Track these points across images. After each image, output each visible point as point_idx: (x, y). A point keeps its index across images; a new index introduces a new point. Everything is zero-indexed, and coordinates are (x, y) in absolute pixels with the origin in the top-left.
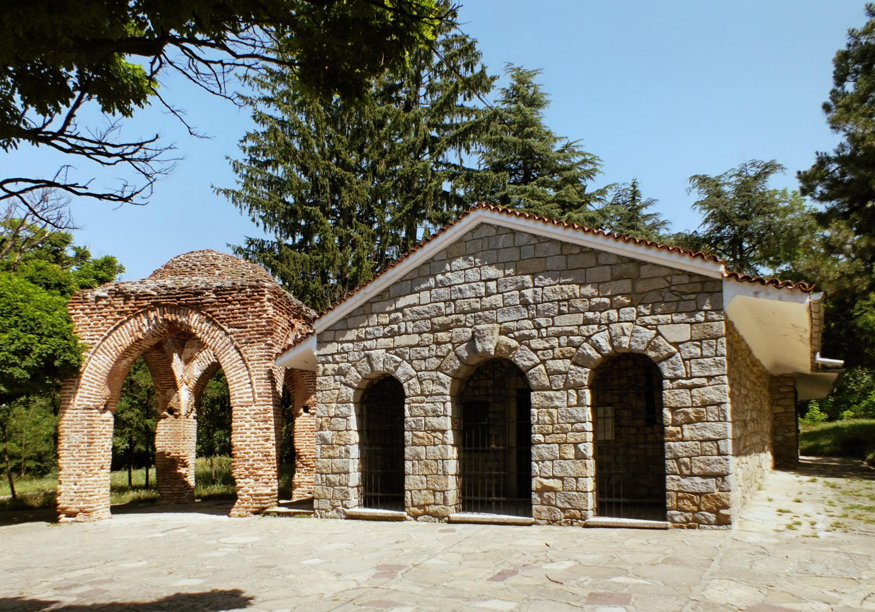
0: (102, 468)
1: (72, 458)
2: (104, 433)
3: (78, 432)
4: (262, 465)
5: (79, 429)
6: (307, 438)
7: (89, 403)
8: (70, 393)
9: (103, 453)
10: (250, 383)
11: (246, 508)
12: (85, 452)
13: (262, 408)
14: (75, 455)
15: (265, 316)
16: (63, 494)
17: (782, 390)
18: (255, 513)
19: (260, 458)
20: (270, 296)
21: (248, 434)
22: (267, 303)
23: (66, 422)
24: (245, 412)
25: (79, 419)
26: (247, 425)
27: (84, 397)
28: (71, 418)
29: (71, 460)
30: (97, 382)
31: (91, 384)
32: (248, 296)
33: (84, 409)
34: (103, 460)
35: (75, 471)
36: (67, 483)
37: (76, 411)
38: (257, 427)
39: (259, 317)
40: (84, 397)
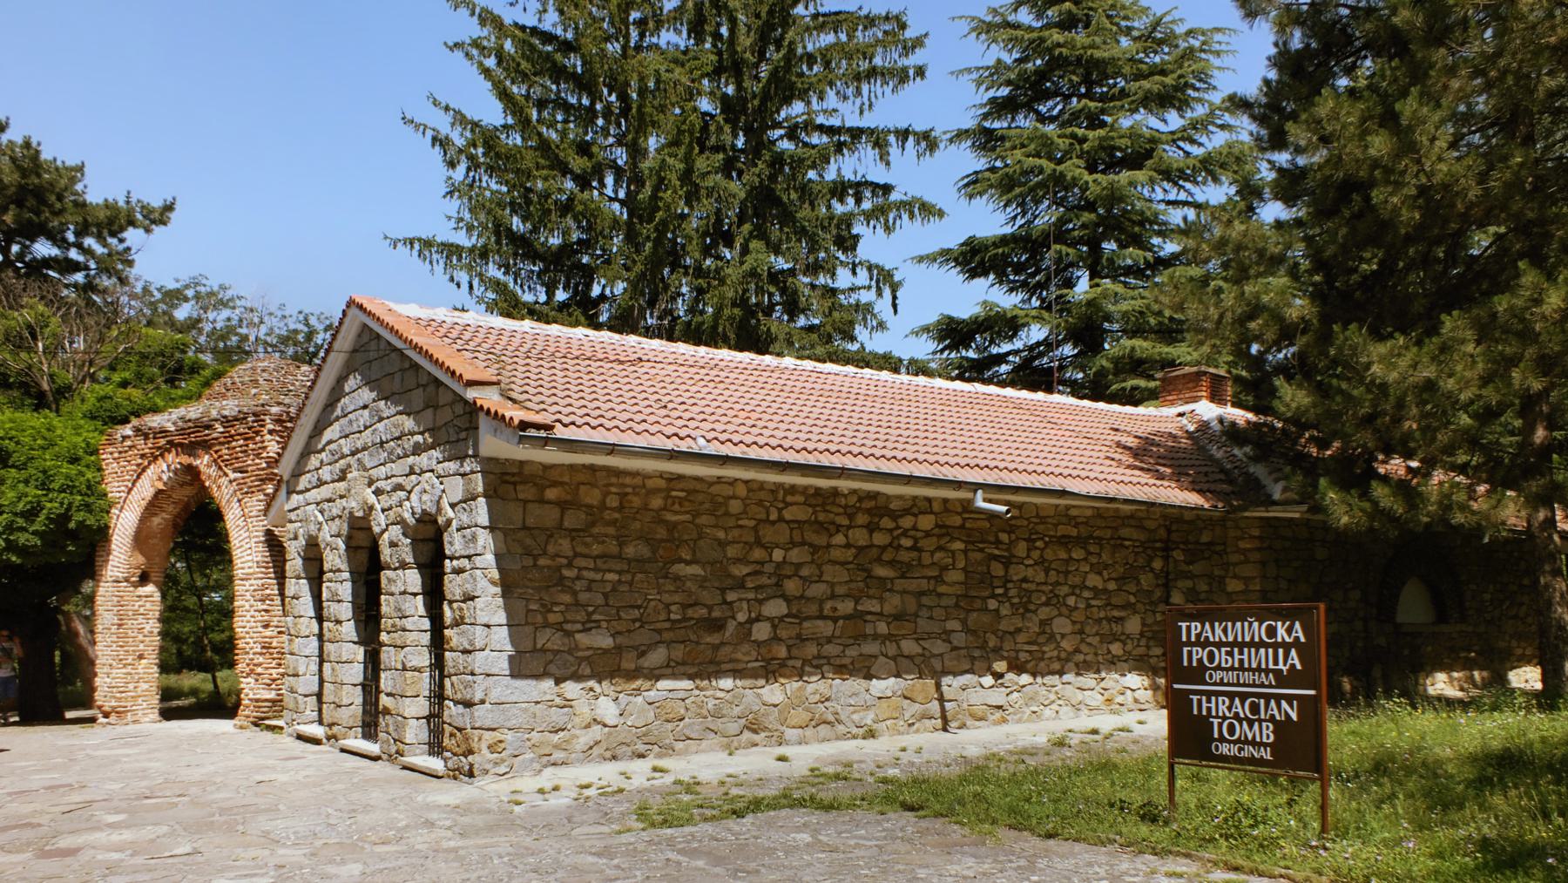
0: (141, 657)
2: (142, 610)
4: (261, 659)
9: (141, 637)
11: (248, 717)
13: (260, 582)
15: (264, 455)
17: (1242, 545)
18: (256, 725)
19: (259, 650)
20: (271, 427)
21: (248, 618)
22: (268, 437)
26: (247, 605)
32: (249, 428)
34: (141, 647)
39: (258, 456)
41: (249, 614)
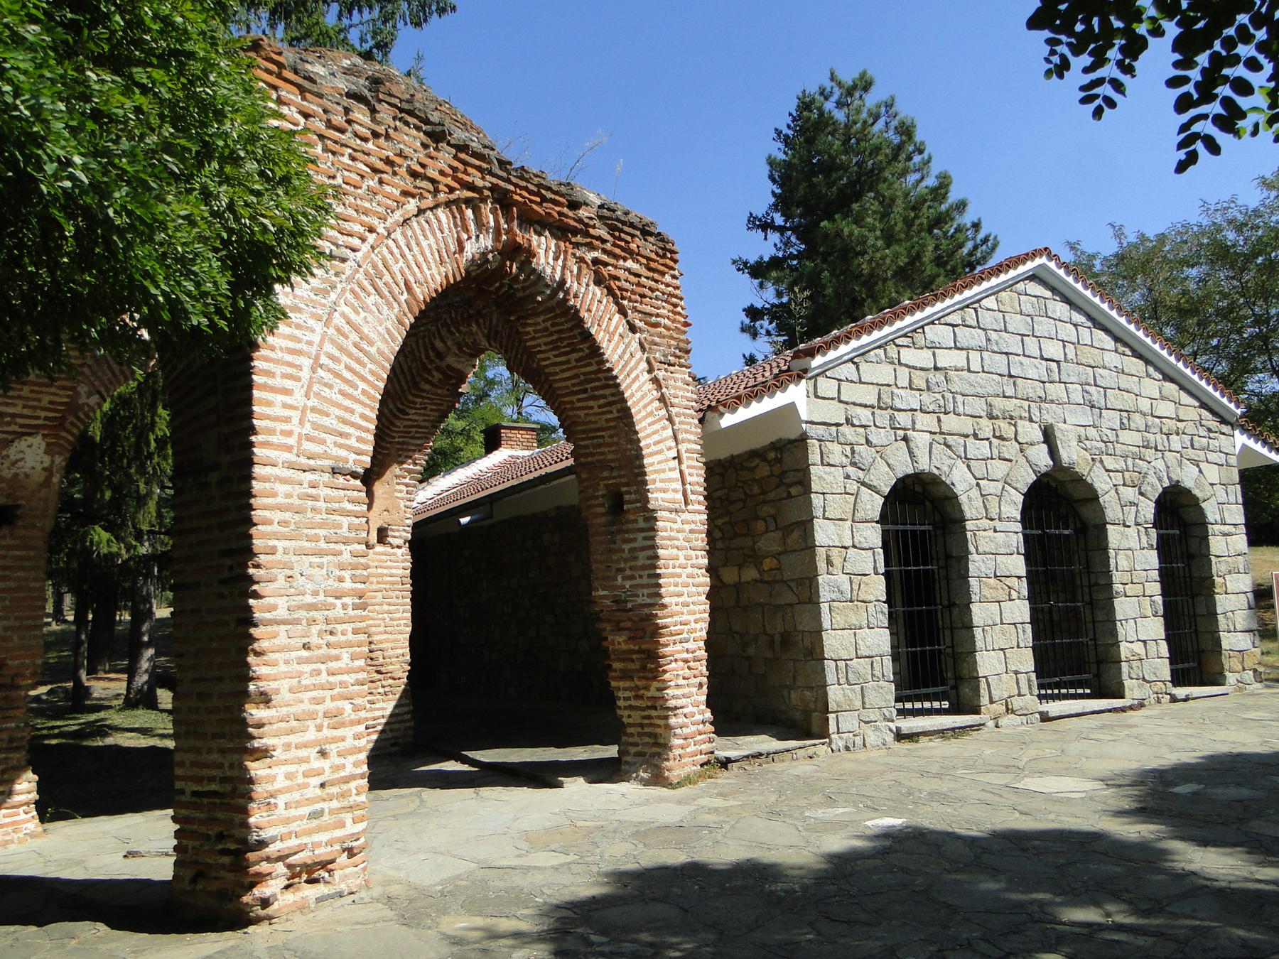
1: (305, 653)
3: (320, 553)
5: (322, 545)
6: (386, 607)
7: (343, 453)
8: (286, 406)
10: (678, 458)
12: (349, 627)
14: (314, 640)
16: (281, 800)
23: (277, 516)
24: (675, 526)
25: (321, 504)
27: (328, 431)
28: (295, 501)
29: (301, 661)
30: (362, 385)
31: (346, 388)
33: (334, 472)
35: (321, 701)
36: (294, 753)
37: (309, 476)
38: (694, 561)
40: (328, 431)
41: (684, 572)
